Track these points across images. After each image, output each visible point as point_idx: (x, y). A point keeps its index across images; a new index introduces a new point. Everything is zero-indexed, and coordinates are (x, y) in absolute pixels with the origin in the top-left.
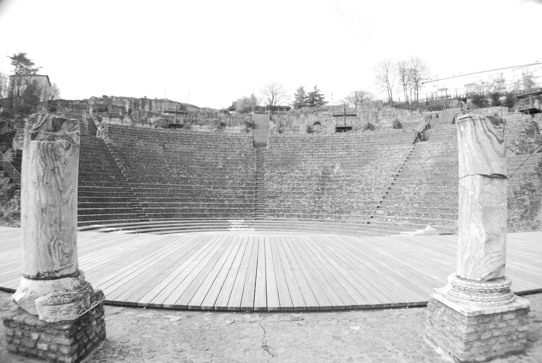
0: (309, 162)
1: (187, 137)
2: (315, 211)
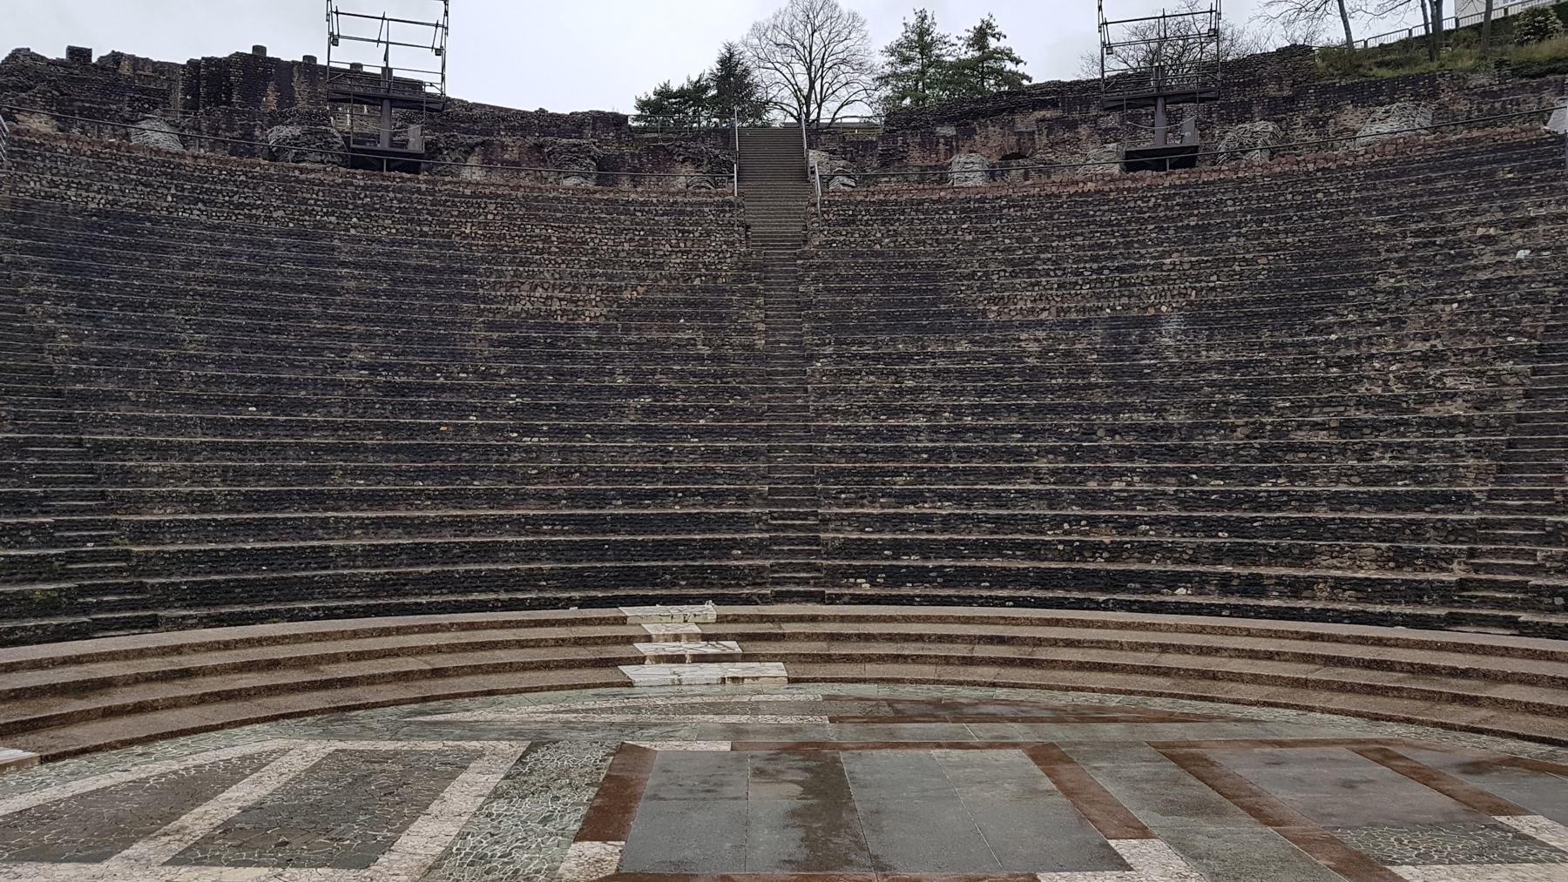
0: (1021, 305)
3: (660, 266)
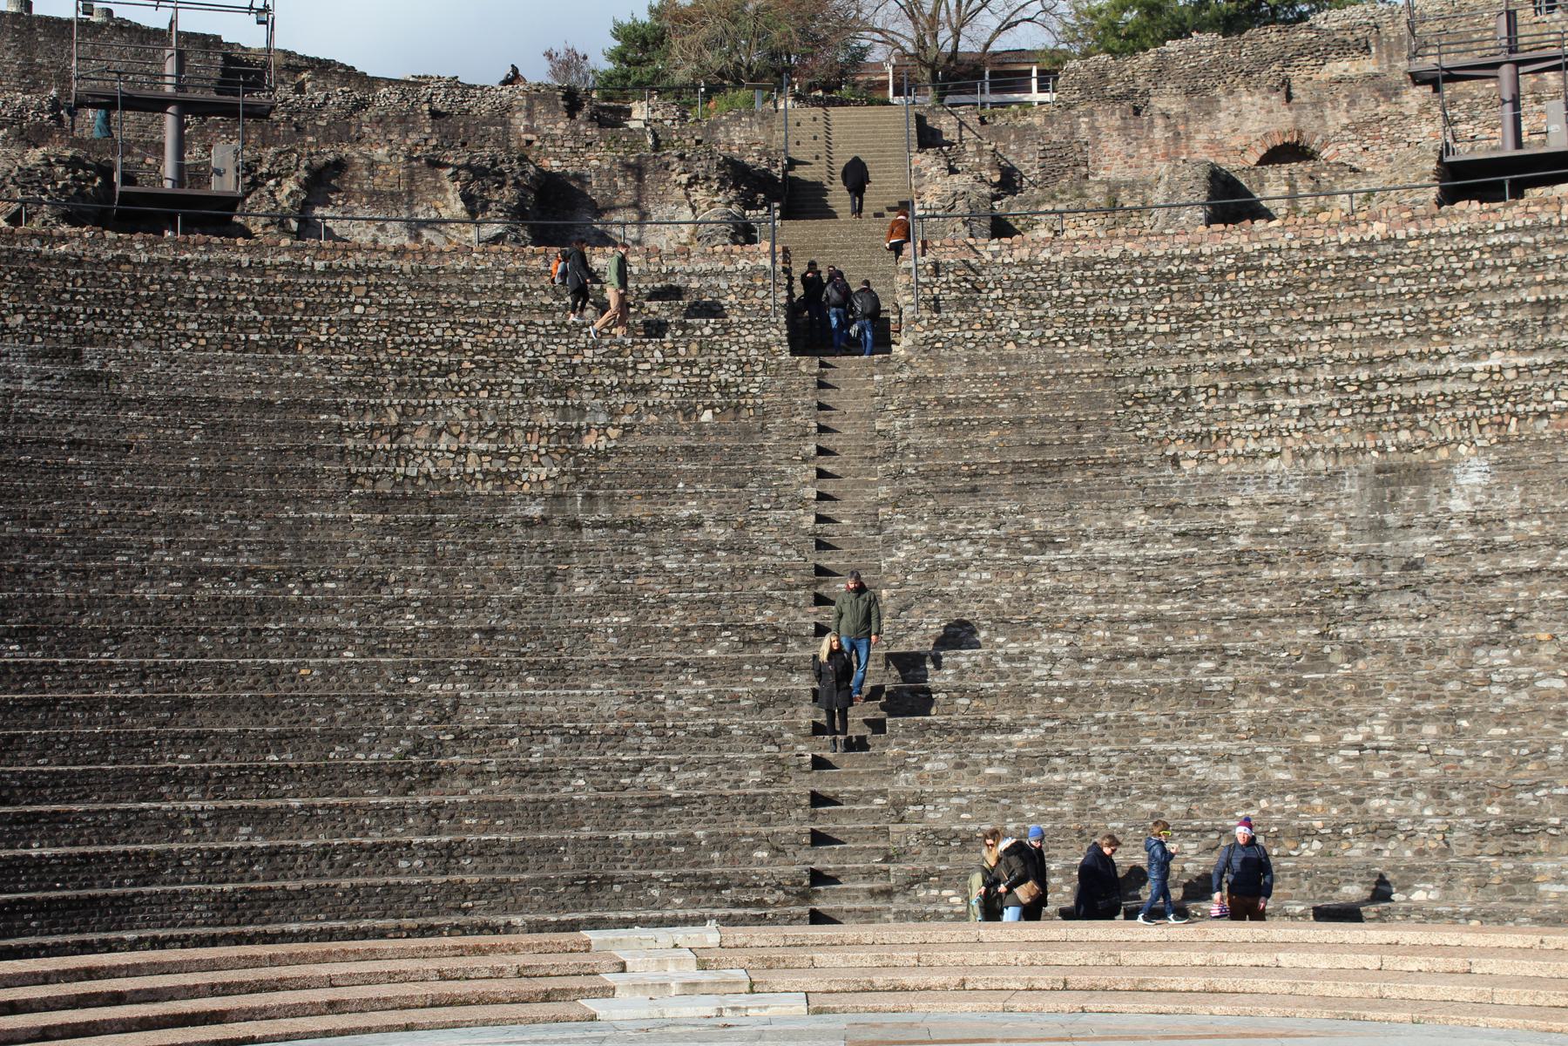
0: (1238, 445)
1: (267, 288)
2: (1305, 834)
3: (646, 389)
